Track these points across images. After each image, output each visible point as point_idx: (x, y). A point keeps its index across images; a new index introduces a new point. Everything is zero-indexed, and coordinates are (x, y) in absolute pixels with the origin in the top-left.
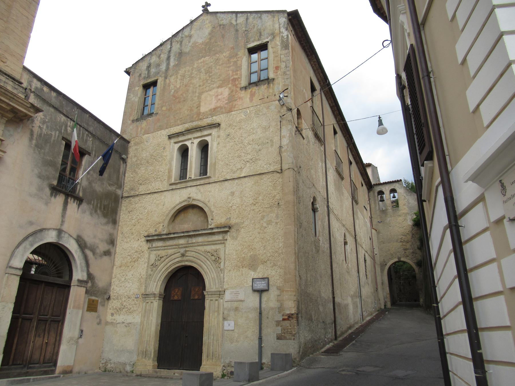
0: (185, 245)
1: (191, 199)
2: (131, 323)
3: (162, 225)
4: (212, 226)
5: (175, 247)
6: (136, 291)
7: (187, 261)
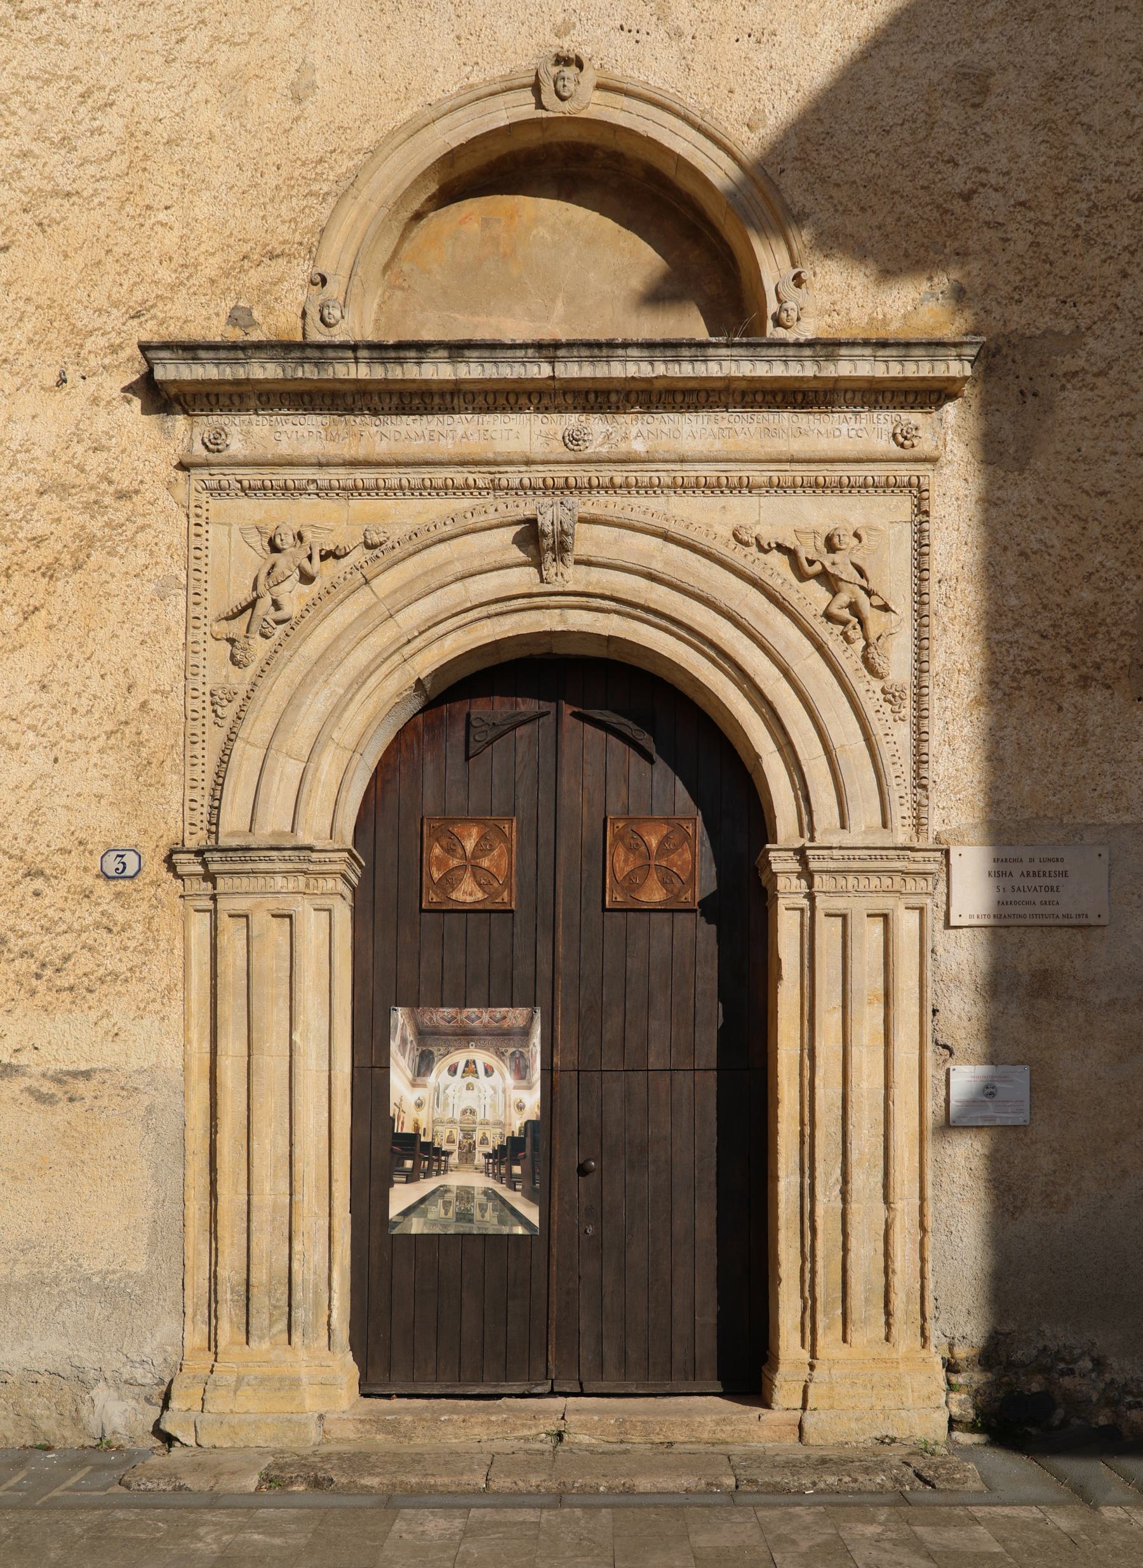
0: (560, 473)
1: (589, 77)
2: (87, 1075)
3: (302, 270)
4: (807, 330)
5: (459, 476)
6: (105, 823)
7: (587, 599)
